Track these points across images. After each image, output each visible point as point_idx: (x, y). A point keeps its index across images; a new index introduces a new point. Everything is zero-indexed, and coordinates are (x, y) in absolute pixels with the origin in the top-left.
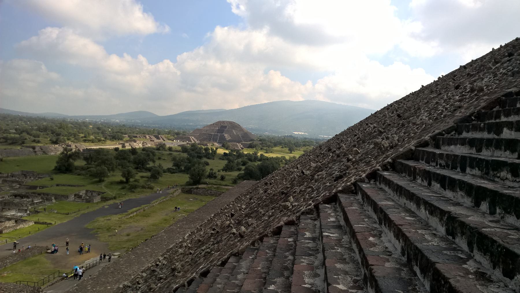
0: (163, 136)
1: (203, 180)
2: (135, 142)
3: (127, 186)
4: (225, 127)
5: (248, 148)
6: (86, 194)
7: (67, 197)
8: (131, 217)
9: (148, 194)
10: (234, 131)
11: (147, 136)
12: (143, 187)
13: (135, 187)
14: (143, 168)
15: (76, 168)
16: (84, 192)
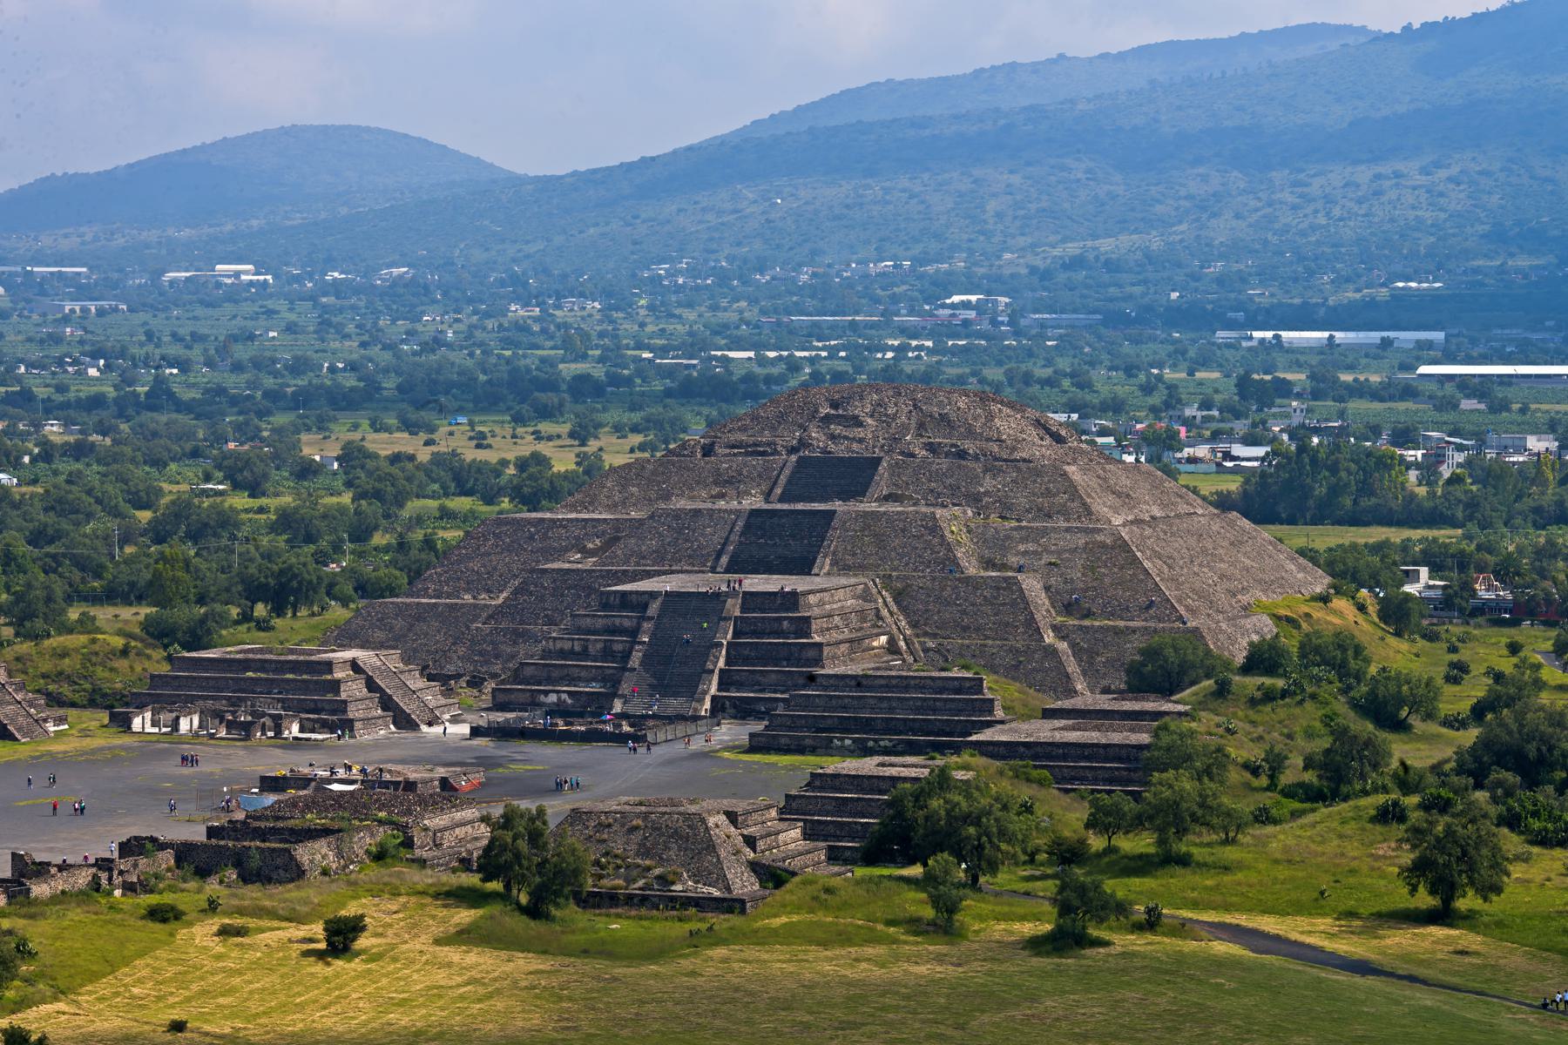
4: (854, 476)
5: (870, 858)
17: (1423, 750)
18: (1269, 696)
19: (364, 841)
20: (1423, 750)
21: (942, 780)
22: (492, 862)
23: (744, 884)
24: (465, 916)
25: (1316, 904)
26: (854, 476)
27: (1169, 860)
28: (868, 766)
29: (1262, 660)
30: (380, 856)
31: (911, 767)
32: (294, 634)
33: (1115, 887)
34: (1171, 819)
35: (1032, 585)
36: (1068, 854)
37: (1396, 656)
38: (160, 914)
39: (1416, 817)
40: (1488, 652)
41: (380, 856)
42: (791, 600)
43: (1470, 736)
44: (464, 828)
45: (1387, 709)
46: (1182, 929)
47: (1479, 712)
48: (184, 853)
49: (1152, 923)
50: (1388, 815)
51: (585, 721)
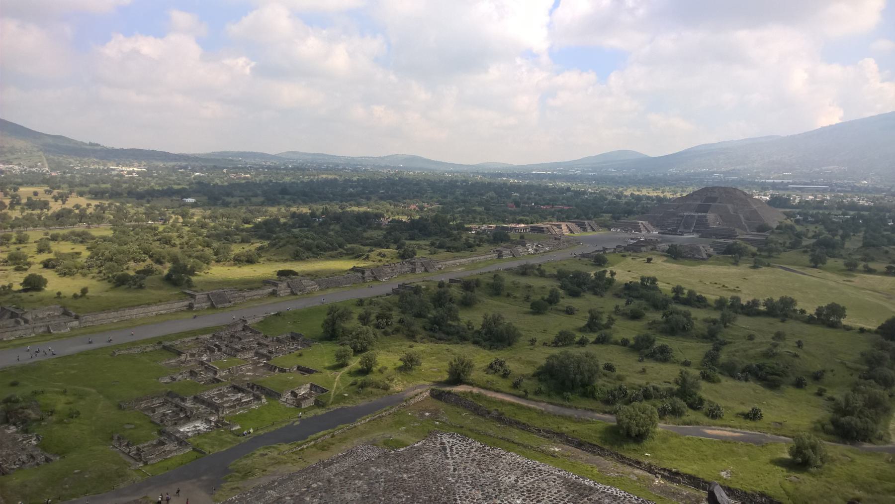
0: (593, 223)
1: (474, 376)
2: (524, 245)
3: (360, 379)
4: (714, 200)
5: (723, 253)
6: (311, 389)
7: (279, 396)
8: (302, 449)
9: (374, 399)
10: (730, 206)
11: (563, 225)
12: (377, 386)
13: (363, 386)
14: (440, 329)
15: (345, 332)
16: (308, 386)
17: (806, 242)
18: (780, 233)
19: (650, 247)
20: (806, 242)
21: (735, 243)
22: (668, 252)
23: (705, 256)
24: (665, 258)
25: (794, 264)
26: (714, 200)
27: (770, 257)
28: (722, 240)
29: (778, 228)
30: (652, 250)
31: (728, 241)
32: (631, 219)
33: (765, 260)
34: (770, 251)
35: (741, 216)
36: (754, 255)
37: (798, 228)
38: (624, 256)
39: (810, 253)
40: (812, 228)
41: (652, 250)
42: (705, 217)
43: (814, 240)
44: (665, 246)
45: (799, 236)
46: (773, 267)
47: (813, 237)
48: (625, 248)
49: (768, 265)
50: (805, 252)
51: (674, 232)
